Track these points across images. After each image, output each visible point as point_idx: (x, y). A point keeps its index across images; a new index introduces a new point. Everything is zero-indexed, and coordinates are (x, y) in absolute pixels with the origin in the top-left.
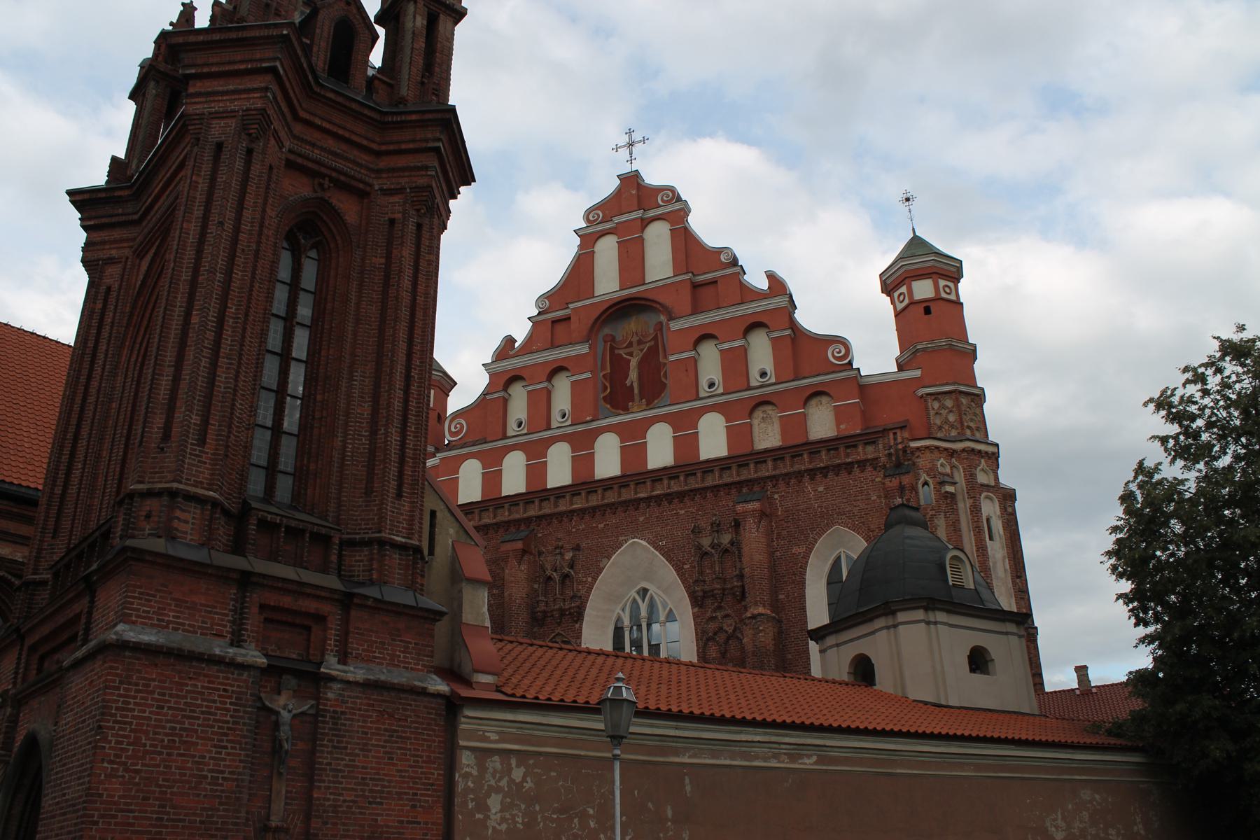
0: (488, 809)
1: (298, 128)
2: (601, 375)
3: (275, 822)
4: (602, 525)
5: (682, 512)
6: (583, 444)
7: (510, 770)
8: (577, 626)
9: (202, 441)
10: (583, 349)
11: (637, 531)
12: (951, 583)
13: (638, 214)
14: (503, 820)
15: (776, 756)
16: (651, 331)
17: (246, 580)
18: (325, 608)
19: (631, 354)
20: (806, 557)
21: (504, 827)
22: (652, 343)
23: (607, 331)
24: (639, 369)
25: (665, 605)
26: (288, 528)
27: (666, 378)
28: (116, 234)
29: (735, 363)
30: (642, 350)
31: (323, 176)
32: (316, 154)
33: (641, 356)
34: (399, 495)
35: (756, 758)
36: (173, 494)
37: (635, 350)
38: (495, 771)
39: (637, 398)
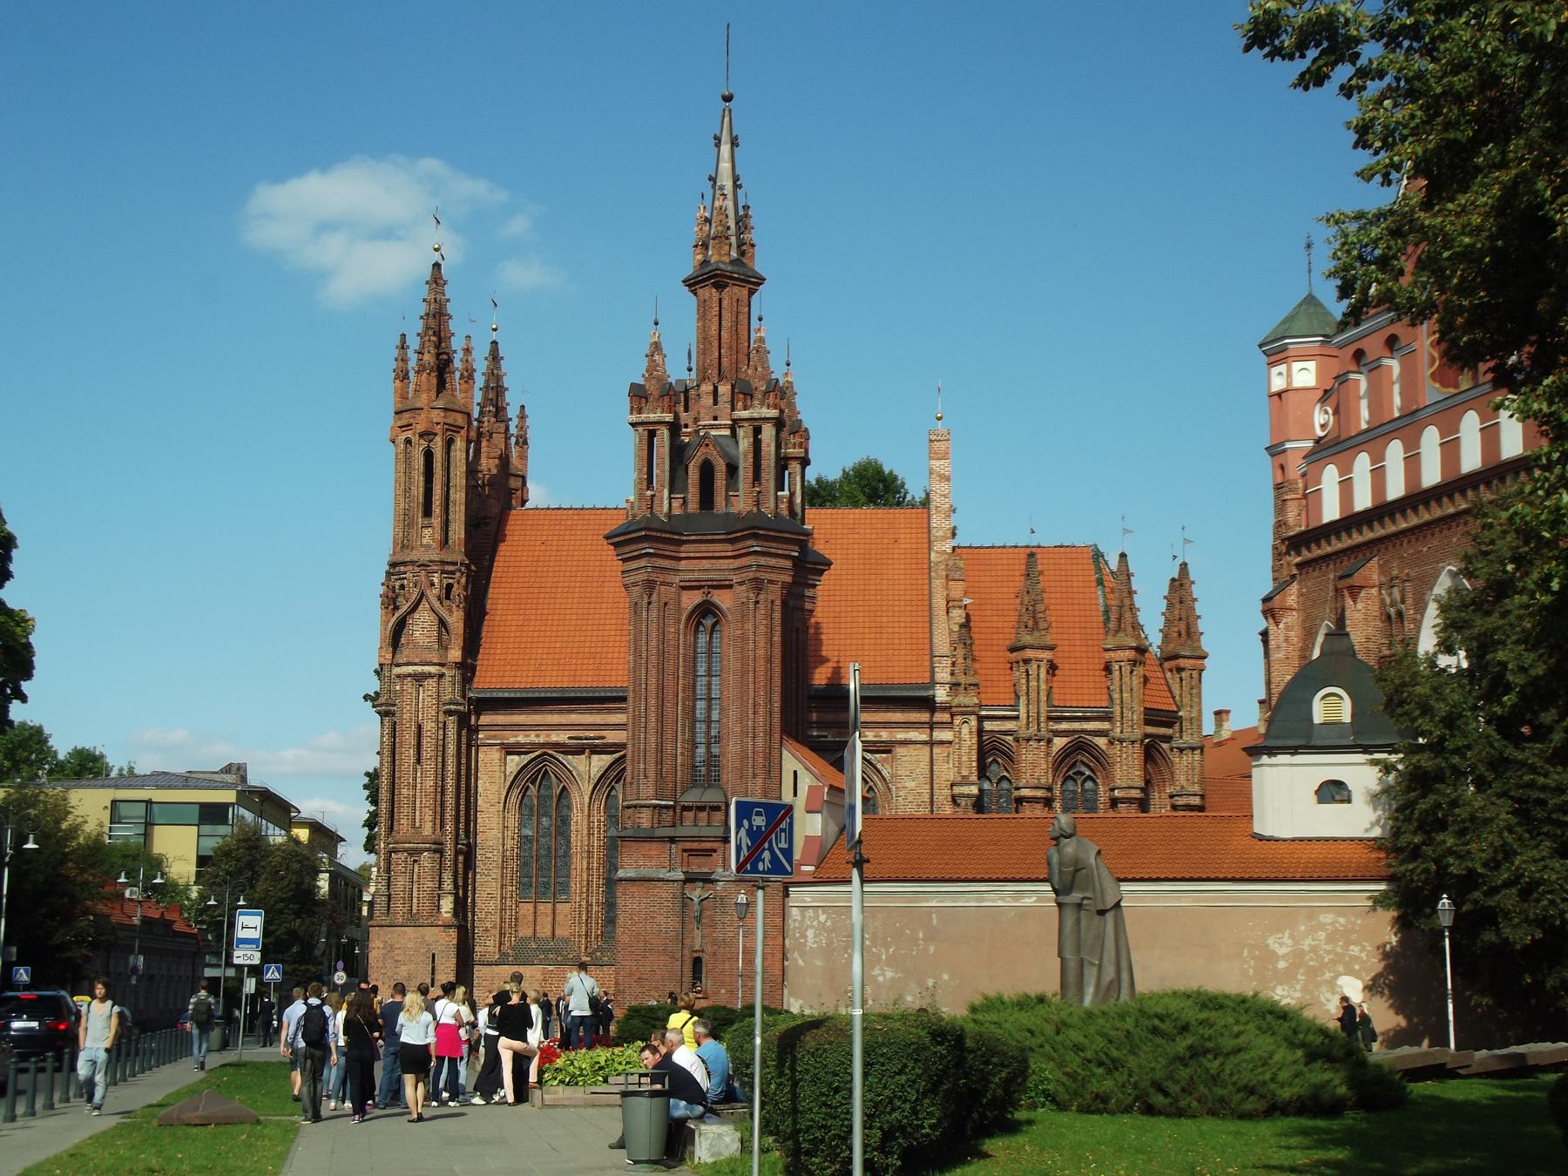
0: (806, 936)
1: (683, 565)
2: (1428, 343)
3: (697, 947)
4: (1425, 549)
7: (818, 916)
9: (646, 777)
12: (1318, 717)
14: (815, 942)
15: (1001, 899)
17: (672, 840)
18: (715, 845)
21: (815, 945)
26: (697, 807)
31: (703, 587)
32: (696, 576)
34: (754, 776)
35: (987, 900)
36: (635, 807)
38: (810, 917)
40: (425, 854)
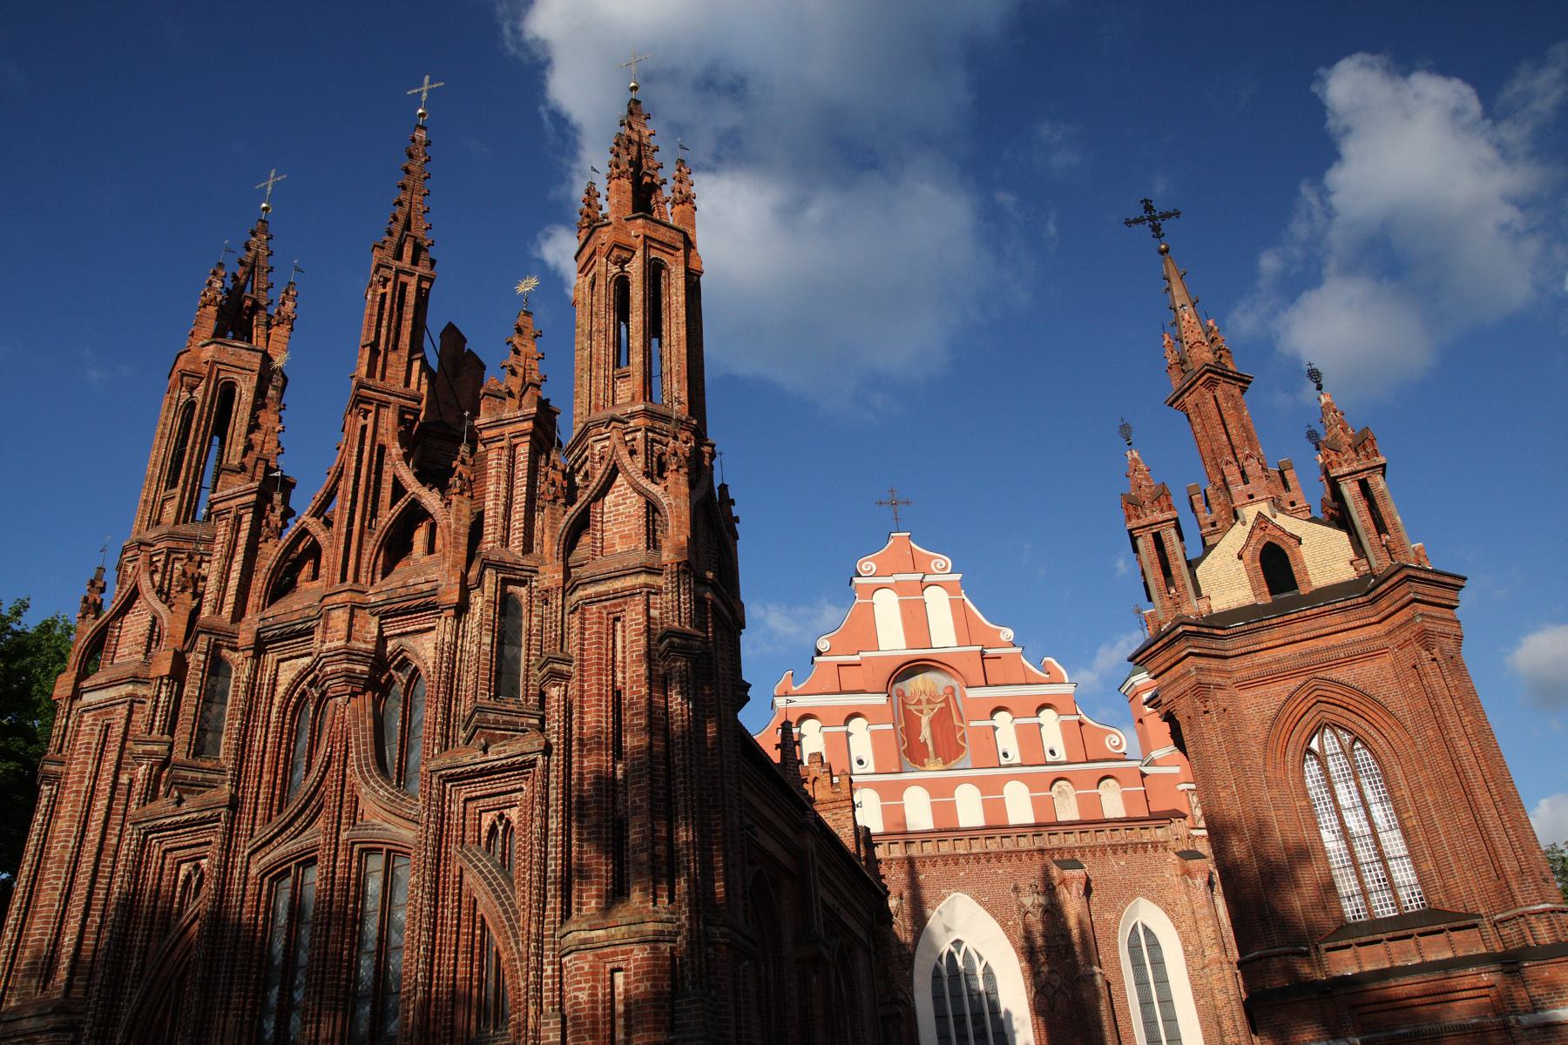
5: (1000, 871)
6: (891, 794)
8: (908, 973)
10: (881, 699)
11: (960, 886)
13: (919, 576)
16: (941, 693)
19: (921, 712)
20: (1117, 922)
22: (943, 705)
23: (898, 685)
24: (931, 728)
25: (981, 958)
27: (965, 742)
28: (1214, 663)
29: (1030, 738)
30: (932, 710)
33: (932, 714)
37: (925, 707)
39: (932, 754)
40: (746, 963)
